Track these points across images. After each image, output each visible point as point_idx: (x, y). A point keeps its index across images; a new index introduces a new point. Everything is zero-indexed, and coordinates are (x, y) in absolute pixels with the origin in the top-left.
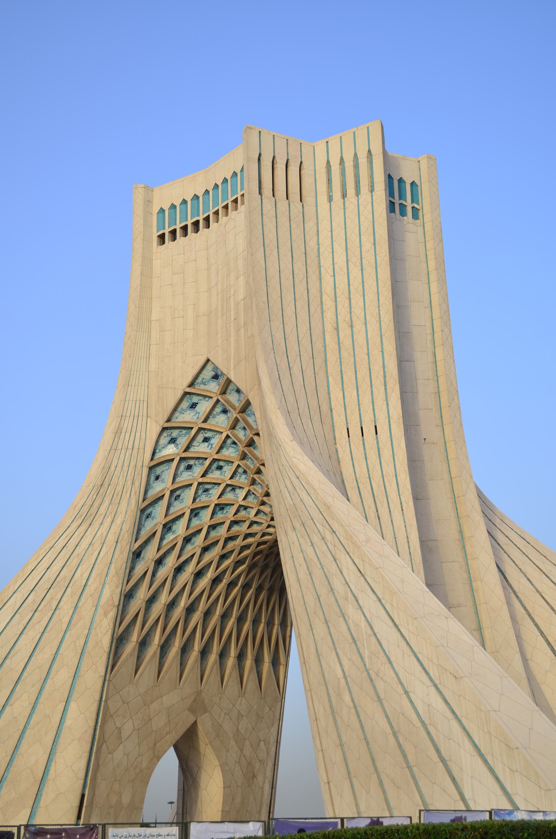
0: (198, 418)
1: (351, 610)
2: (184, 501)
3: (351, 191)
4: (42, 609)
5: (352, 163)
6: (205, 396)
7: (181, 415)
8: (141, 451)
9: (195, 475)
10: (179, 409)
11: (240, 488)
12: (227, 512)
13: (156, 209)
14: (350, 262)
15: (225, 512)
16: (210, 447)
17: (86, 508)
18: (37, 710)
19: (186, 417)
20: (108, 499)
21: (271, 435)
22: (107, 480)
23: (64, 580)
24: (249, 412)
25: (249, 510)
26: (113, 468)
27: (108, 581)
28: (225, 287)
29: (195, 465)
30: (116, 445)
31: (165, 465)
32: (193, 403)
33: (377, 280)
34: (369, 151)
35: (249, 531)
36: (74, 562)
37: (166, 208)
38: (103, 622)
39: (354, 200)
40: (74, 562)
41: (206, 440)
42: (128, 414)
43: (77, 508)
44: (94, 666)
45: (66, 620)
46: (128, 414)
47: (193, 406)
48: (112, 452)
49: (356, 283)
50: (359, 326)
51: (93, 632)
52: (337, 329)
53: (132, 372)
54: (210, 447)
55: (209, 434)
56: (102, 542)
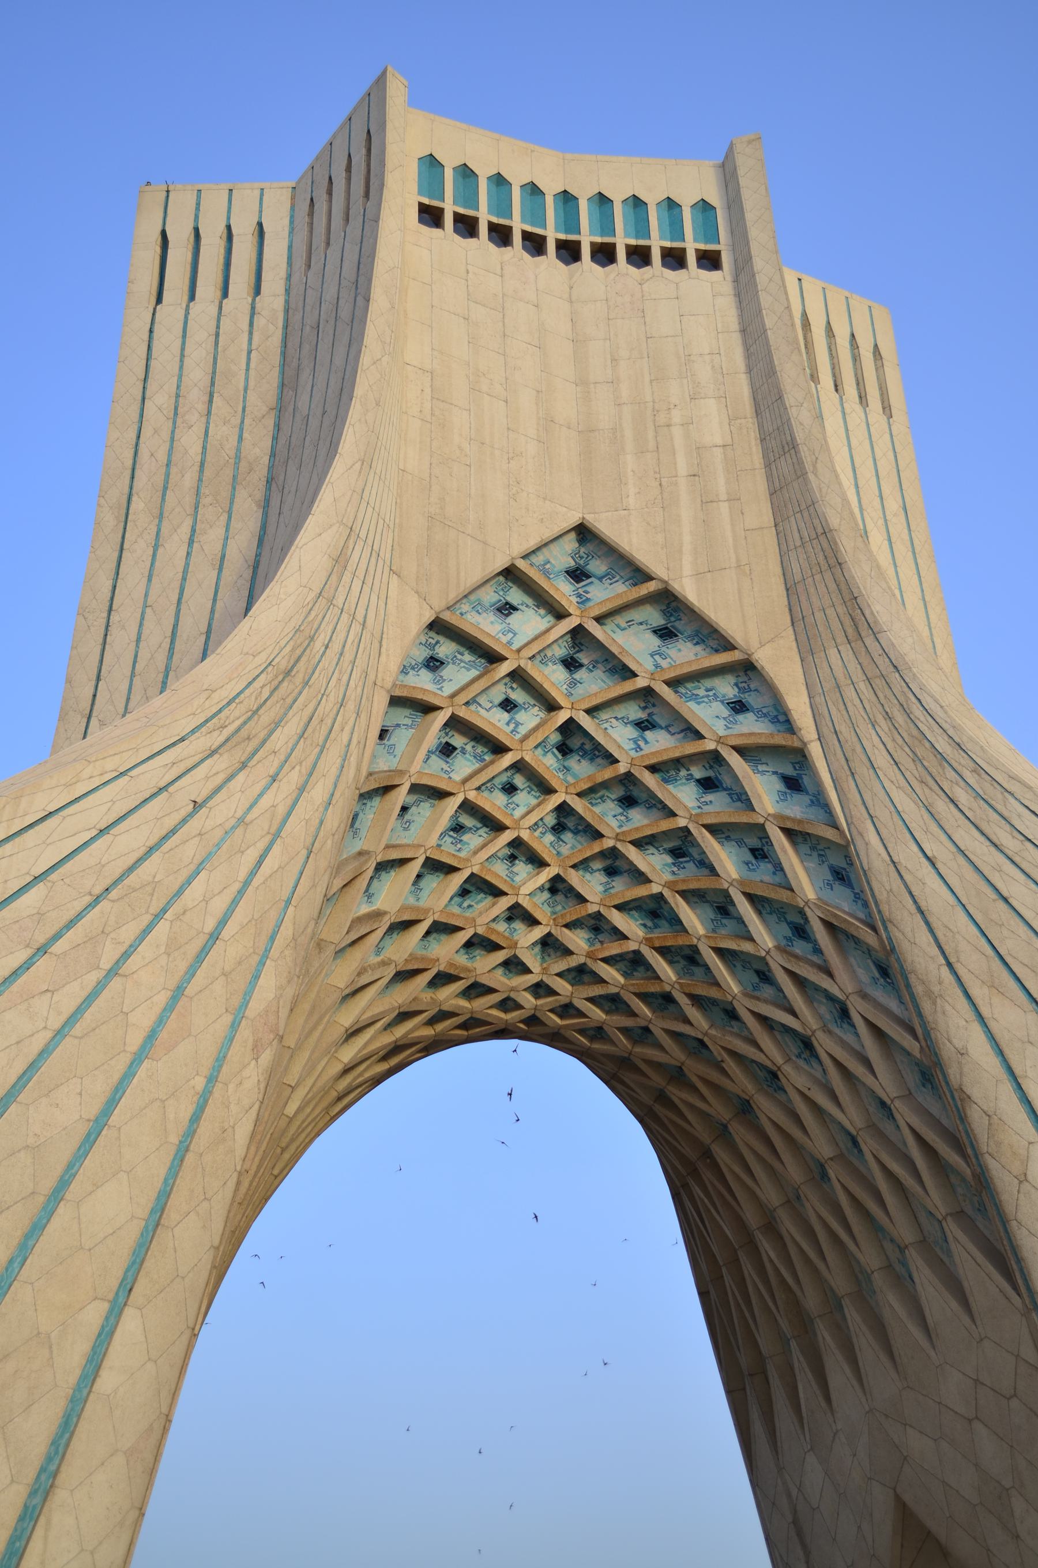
0: (510, 643)
2: (413, 828)
4: (65, 953)
5: (847, 345)
7: (474, 613)
9: (457, 777)
10: (472, 597)
12: (470, 906)
14: (865, 513)
15: (465, 904)
16: (512, 726)
17: (236, 713)
19: (487, 627)
20: (296, 719)
21: (937, 760)
22: (301, 665)
23: (149, 889)
24: (702, 692)
25: (518, 925)
27: (274, 953)
28: (649, 398)
29: (463, 751)
30: (332, 591)
31: (407, 712)
32: (507, 603)
33: (920, 577)
34: (876, 346)
35: (485, 980)
36: (186, 850)
37: (450, 163)
38: (246, 1073)
39: (858, 408)
41: (508, 705)
42: (363, 535)
43: (216, 697)
44: (205, 1204)
45: (143, 1019)
46: (363, 535)
47: (507, 609)
48: (322, 602)
53: (379, 443)
54: (512, 726)
56: (273, 830)
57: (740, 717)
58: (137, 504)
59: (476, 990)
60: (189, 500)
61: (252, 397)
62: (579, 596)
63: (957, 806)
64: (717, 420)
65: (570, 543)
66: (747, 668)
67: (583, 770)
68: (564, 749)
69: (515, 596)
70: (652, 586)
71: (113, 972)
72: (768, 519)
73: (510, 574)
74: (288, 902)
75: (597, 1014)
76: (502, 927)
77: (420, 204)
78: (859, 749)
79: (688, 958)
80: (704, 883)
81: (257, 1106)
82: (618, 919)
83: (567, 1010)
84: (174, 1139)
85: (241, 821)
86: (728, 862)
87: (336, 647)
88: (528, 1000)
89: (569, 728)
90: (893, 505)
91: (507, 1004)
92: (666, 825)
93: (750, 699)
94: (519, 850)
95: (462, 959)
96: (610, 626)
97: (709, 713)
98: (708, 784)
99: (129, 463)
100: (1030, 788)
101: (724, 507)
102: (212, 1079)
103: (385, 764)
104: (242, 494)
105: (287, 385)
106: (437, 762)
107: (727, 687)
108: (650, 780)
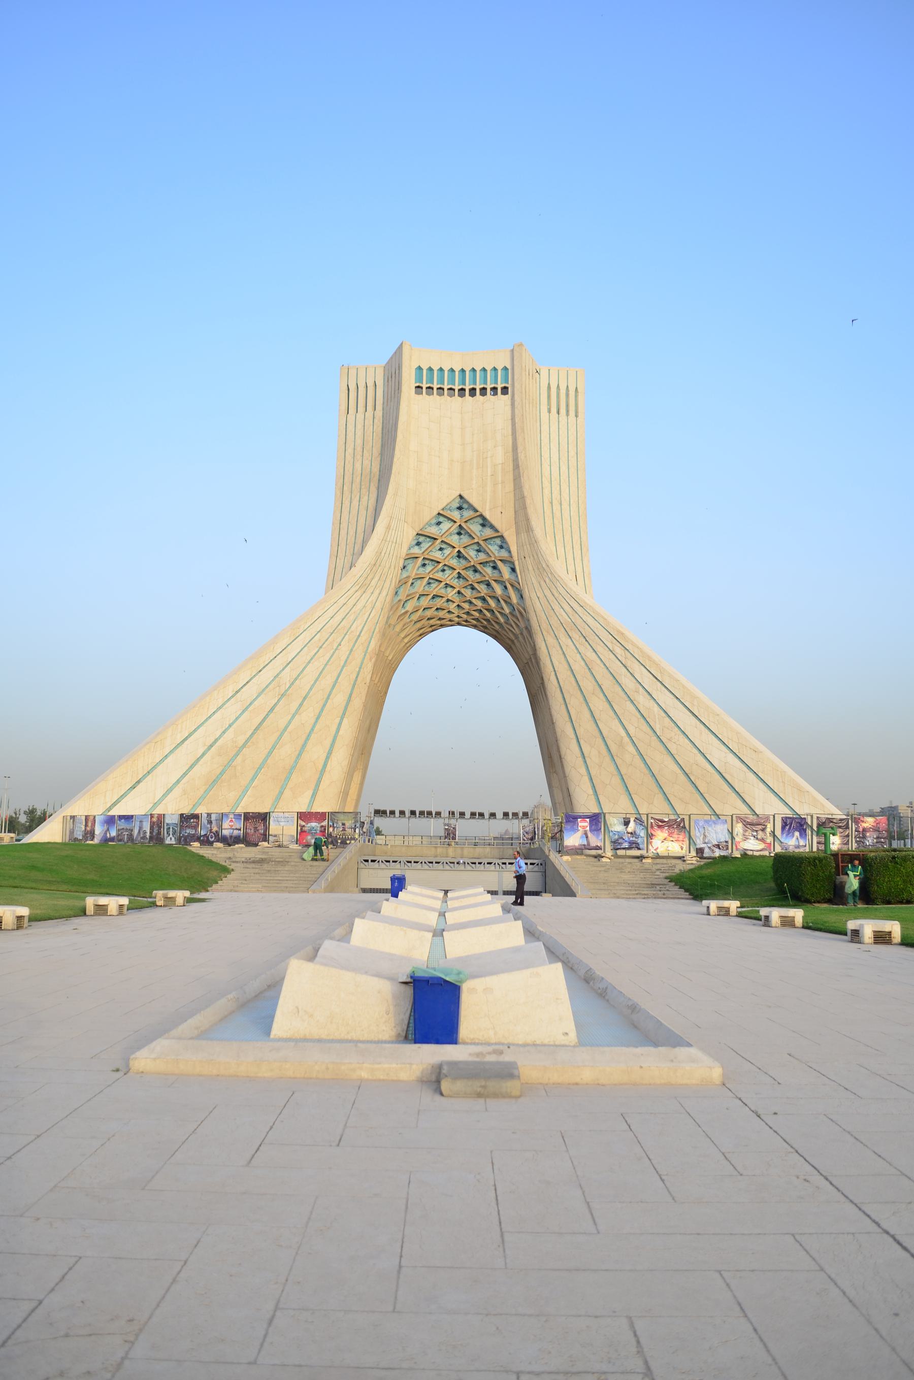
1: (642, 700)
6: (449, 519)
11: (452, 587)
17: (362, 579)
18: (320, 721)
19: (433, 531)
21: (543, 569)
26: (383, 554)
36: (351, 617)
40: (351, 617)
41: (441, 549)
45: (344, 658)
47: (439, 523)
49: (564, 476)
50: (565, 506)
52: (552, 503)
55: (444, 546)
58: (345, 488)
59: (440, 619)
60: (358, 487)
64: (500, 455)
65: (458, 500)
66: (502, 537)
67: (463, 562)
68: (459, 557)
69: (441, 519)
70: (478, 514)
71: (336, 649)
72: (512, 488)
73: (439, 514)
75: (474, 622)
76: (445, 604)
79: (491, 611)
80: (493, 594)
82: (474, 601)
83: (466, 621)
86: (498, 590)
88: (457, 619)
89: (459, 552)
90: (572, 453)
91: (450, 621)
92: (483, 579)
93: (504, 545)
94: (447, 585)
95: (436, 613)
96: (468, 524)
97: (493, 548)
98: (495, 568)
101: (500, 486)
102: (360, 668)
103: (405, 575)
104: (372, 484)
105: (383, 446)
106: (421, 569)
107: (498, 541)
108: (478, 567)
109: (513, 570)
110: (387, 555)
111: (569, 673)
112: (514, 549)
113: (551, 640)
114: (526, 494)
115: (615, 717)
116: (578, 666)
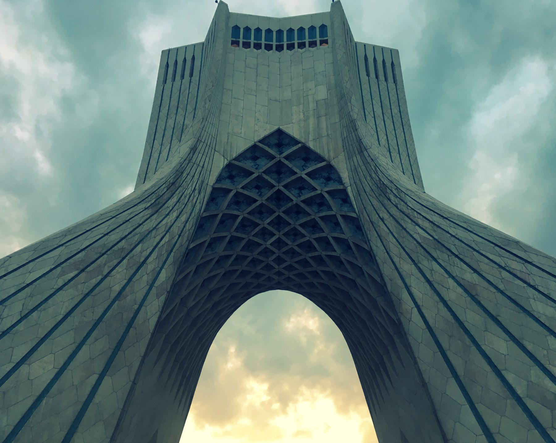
3: (381, 77)
8: (209, 173)
13: (232, 24)
19: (248, 165)
20: (176, 197)
26: (185, 175)
27: (166, 267)
42: (203, 141)
45: (117, 288)
46: (203, 141)
47: (255, 158)
51: (143, 309)
57: (329, 182)
61: (189, 107)
62: (280, 151)
63: (390, 201)
70: (300, 145)
74: (171, 251)
77: (232, 41)
78: (361, 187)
81: (158, 313)
84: (126, 324)
85: (155, 228)
87: (192, 174)
88: (276, 277)
90: (395, 111)
93: (332, 176)
99: (154, 131)
100: (413, 192)
101: (323, 119)
102: (141, 305)
109: (346, 200)
110: (189, 177)
111: (441, 305)
112: (345, 175)
113: (407, 267)
114: (355, 116)
115: (531, 362)
116: (453, 294)
